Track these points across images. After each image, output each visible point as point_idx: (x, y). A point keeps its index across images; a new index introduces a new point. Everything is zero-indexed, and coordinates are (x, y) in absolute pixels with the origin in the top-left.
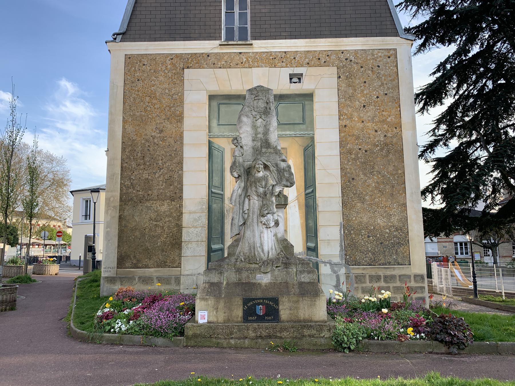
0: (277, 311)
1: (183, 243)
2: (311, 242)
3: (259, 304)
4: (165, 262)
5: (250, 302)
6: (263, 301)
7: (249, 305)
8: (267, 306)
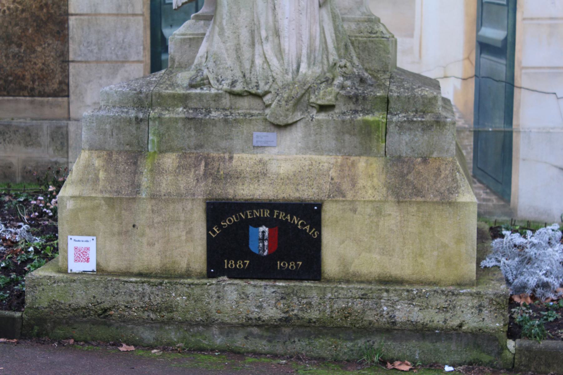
0: (315, 246)
1: (72, 21)
2: (495, 24)
3: (258, 222)
4: (17, 77)
6: (272, 214)
7: (225, 224)
8: (281, 230)
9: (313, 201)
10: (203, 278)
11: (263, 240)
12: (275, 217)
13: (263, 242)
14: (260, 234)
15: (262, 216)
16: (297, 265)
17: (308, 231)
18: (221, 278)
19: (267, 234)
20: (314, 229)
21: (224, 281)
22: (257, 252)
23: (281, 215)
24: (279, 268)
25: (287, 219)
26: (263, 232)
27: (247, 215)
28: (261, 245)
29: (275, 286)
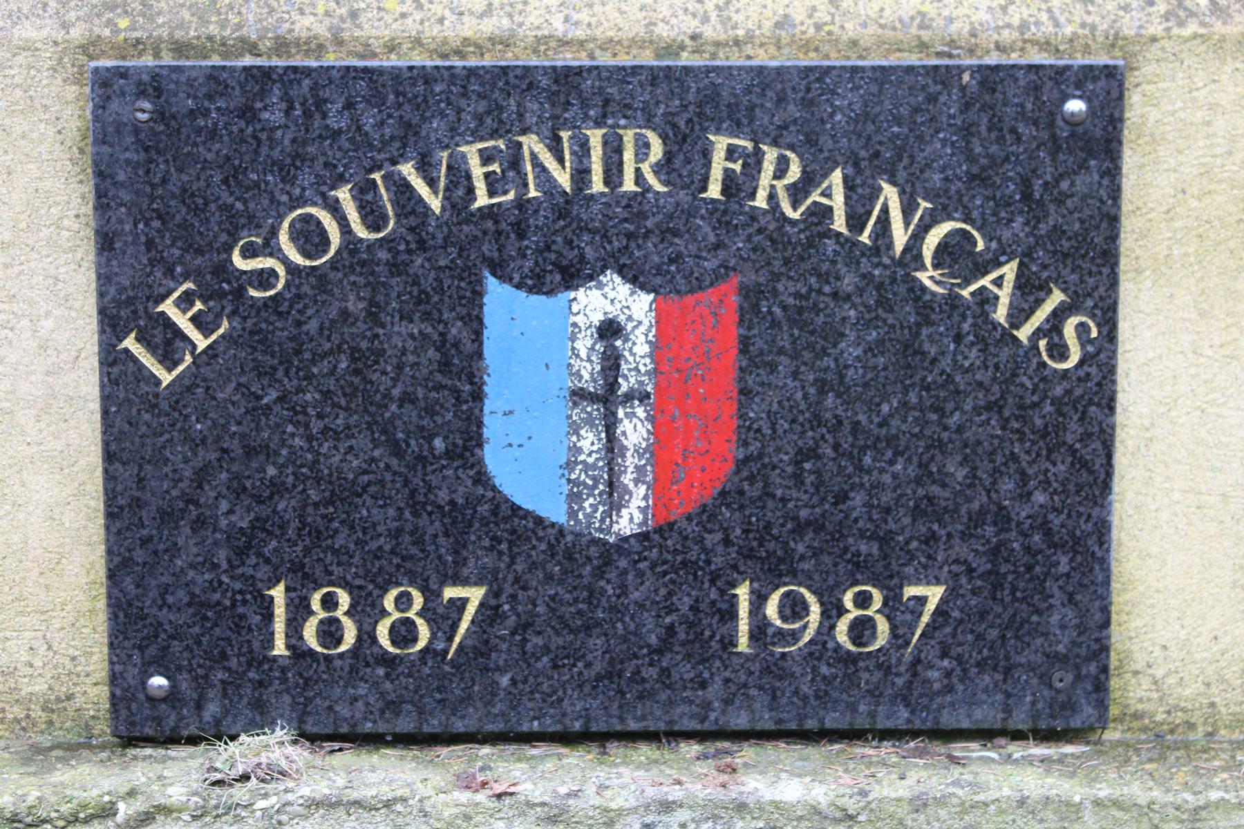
0: (1071, 429)
3: (556, 249)
7: (272, 262)
8: (777, 298)
9: (1046, 45)
10: (76, 747)
11: (605, 398)
12: (714, 191)
13: (611, 426)
14: (584, 344)
15: (597, 185)
17: (1001, 314)
18: (243, 751)
19: (638, 350)
20: (1057, 297)
21: (275, 774)
22: (555, 511)
23: (765, 179)
24: (743, 644)
26: (610, 330)
27: (459, 176)
28: (590, 441)
29: (741, 807)
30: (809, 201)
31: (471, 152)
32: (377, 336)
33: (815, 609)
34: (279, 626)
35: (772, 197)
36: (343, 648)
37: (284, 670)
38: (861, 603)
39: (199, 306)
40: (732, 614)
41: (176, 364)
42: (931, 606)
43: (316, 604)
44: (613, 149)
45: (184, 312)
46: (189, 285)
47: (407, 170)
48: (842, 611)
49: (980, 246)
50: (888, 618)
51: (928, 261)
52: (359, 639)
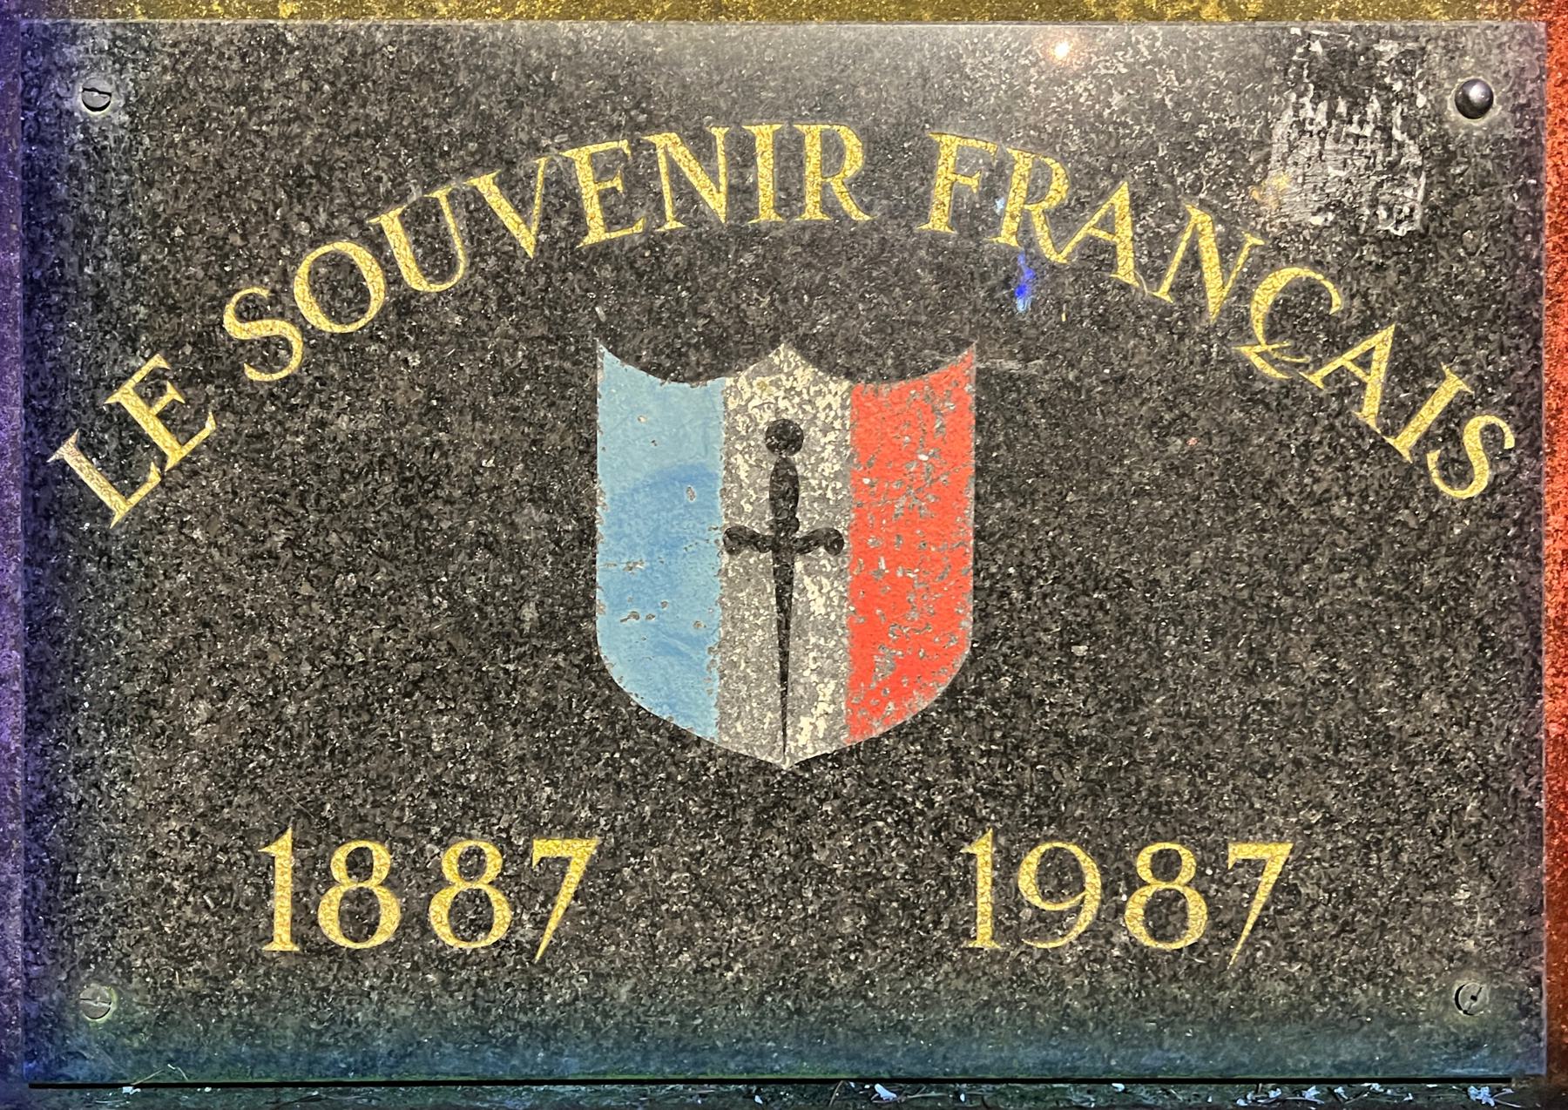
5: (324, 189)
12: (938, 221)
13: (785, 583)
15: (767, 213)
16: (1222, 883)
17: (1369, 411)
19: (823, 466)
20: (1452, 386)
23: (1012, 203)
25: (1099, 256)
26: (786, 437)
27: (564, 196)
30: (1079, 237)
31: (580, 157)
32: (437, 444)
33: (1093, 878)
34: (282, 905)
35: (1025, 229)
36: (378, 939)
37: (285, 974)
38: (1171, 871)
39: (172, 394)
40: (969, 889)
41: (135, 486)
42: (1269, 878)
43: (338, 869)
44: (790, 154)
45: (150, 401)
46: (158, 361)
47: (485, 183)
48: (1134, 883)
49: (1338, 302)
50: (1204, 893)
51: (1259, 330)
52: (403, 926)
